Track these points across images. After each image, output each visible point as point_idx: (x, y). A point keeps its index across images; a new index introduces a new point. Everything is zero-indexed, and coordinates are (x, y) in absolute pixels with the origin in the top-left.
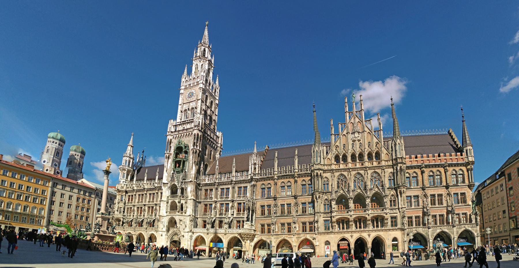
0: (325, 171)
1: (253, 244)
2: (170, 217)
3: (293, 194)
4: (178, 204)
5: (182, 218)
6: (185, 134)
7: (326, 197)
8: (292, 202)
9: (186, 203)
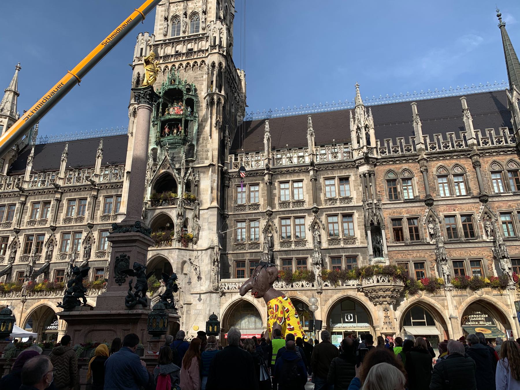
1: (398, 313)
3: (475, 192)
4: (176, 221)
5: (186, 255)
6: (184, 64)
8: (474, 210)
9: (197, 217)
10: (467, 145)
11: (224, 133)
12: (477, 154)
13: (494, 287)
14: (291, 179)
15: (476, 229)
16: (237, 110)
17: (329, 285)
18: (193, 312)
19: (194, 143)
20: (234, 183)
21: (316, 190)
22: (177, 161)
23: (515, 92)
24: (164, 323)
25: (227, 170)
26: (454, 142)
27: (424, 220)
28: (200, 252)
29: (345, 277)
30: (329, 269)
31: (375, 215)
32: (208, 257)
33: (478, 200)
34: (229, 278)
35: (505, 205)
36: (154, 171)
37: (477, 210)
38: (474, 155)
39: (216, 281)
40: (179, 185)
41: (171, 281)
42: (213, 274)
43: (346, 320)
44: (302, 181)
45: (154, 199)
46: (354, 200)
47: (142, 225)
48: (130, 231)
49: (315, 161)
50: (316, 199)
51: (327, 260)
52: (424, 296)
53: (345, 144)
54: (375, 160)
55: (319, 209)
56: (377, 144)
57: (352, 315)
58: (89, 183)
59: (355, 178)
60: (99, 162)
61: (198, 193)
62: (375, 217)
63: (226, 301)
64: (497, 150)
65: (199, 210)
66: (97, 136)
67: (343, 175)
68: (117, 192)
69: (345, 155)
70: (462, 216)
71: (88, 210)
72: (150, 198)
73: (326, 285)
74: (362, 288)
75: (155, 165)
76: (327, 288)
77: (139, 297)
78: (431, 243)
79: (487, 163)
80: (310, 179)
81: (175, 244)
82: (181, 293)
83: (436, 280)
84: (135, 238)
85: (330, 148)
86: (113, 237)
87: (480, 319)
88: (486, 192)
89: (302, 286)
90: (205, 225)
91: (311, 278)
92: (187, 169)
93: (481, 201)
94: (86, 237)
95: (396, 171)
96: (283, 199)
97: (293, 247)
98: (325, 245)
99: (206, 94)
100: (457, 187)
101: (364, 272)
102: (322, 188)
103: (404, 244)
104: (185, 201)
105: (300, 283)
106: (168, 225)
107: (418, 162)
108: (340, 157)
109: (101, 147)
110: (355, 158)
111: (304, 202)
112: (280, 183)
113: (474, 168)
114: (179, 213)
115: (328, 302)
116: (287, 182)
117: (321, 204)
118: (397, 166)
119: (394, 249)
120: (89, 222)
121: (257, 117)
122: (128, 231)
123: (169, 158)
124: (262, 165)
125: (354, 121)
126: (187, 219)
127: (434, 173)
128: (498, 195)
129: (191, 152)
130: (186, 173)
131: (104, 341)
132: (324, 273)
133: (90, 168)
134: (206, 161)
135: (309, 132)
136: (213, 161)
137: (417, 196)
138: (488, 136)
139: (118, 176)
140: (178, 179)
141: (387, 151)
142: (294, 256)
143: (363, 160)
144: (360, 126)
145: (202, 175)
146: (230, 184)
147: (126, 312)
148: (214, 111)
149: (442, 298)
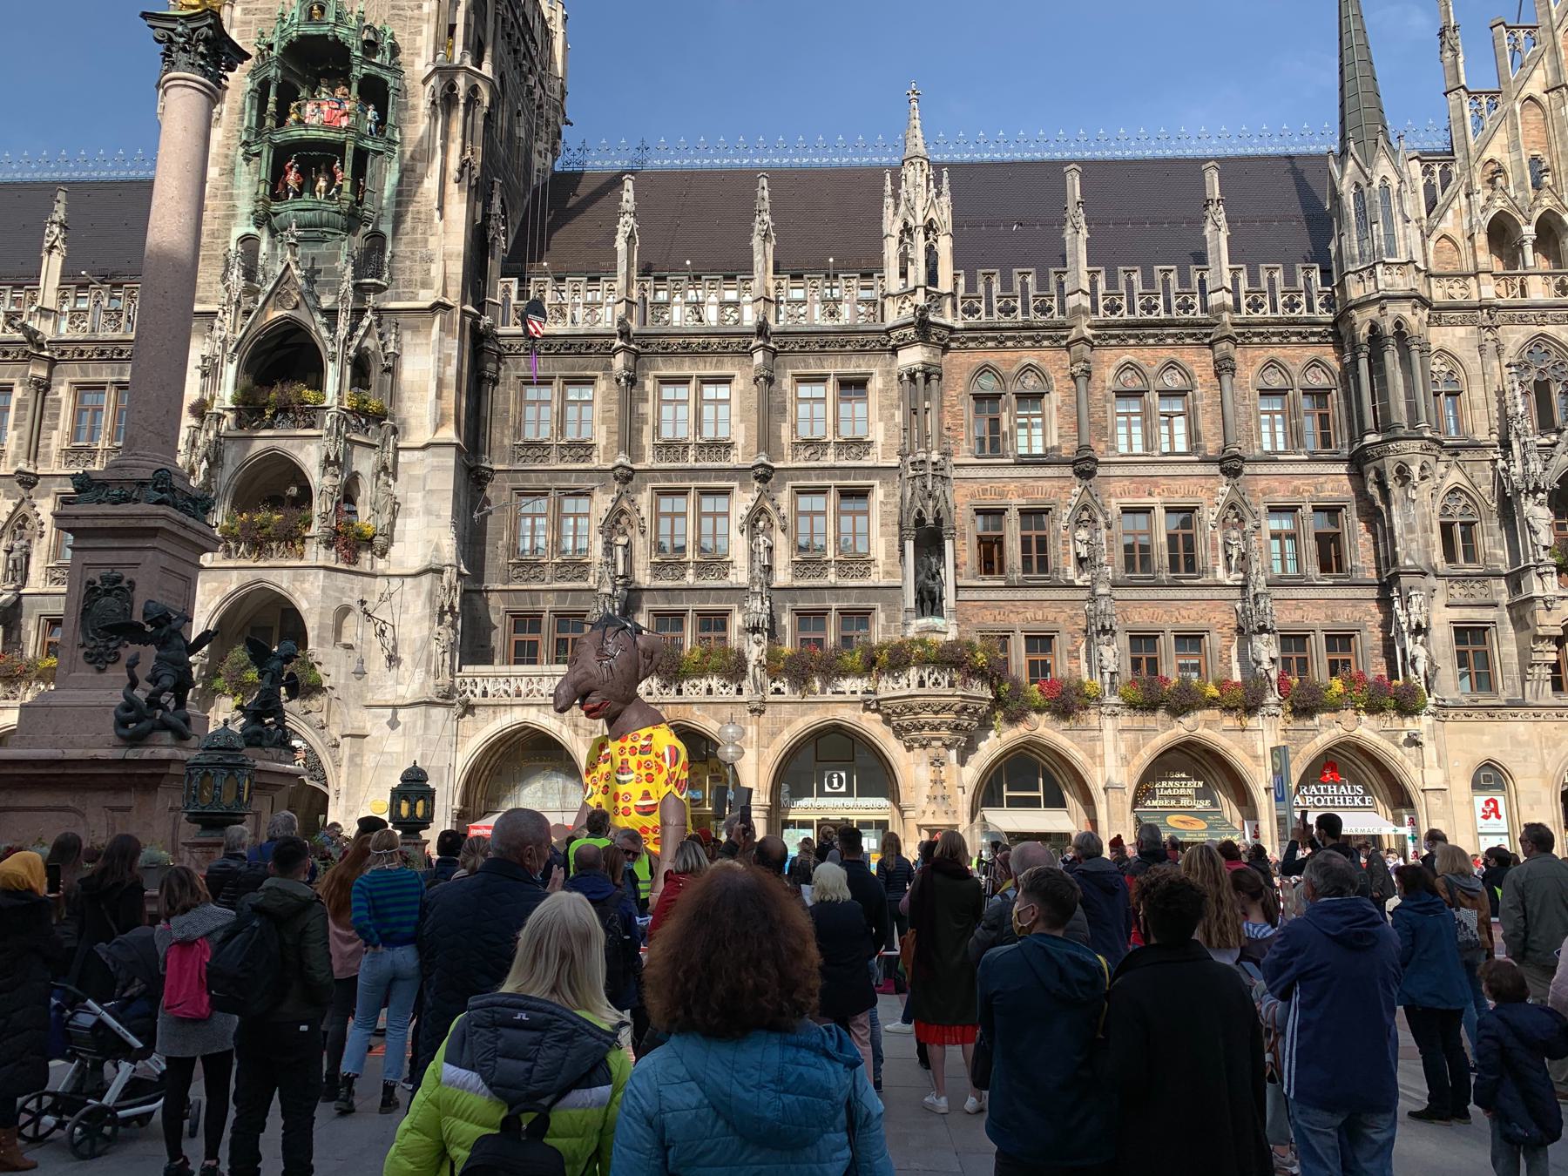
0: (1439, 313)
2: (233, 582)
3: (1212, 446)
4: (318, 479)
5: (351, 589)
7: (1455, 477)
8: (1203, 497)
9: (389, 470)
10: (1205, 309)
11: (487, 205)
12: (1228, 337)
13: (1228, 709)
14: (695, 373)
15: (1201, 551)
16: (533, 134)
17: (786, 689)
18: (369, 760)
19: (386, 228)
20: (512, 371)
21: (769, 412)
22: (327, 283)
23: (1351, 163)
24: (240, 788)
25: (492, 326)
26: (1173, 296)
27: (1065, 518)
28: (396, 582)
29: (832, 670)
30: (788, 647)
31: (930, 496)
32: (423, 596)
33: (1215, 469)
34: (491, 662)
35: (1283, 487)
36: (248, 313)
37: (1210, 496)
38: (1221, 339)
39: (447, 671)
40: (330, 365)
41: (275, 665)
42: (436, 648)
43: (827, 789)
44: (729, 382)
45: (246, 404)
46: (877, 450)
47: (177, 483)
48: (136, 501)
49: (771, 321)
50: (766, 439)
51: (786, 620)
52: (1045, 728)
53: (863, 276)
54: (946, 333)
55: (773, 469)
56: (956, 285)
57: (843, 775)
58: (19, 336)
59: (886, 384)
60: (52, 267)
61: (394, 394)
62: (931, 503)
63: (477, 729)
64: (1282, 329)
65: (397, 449)
66: (46, 176)
67: (851, 370)
68: (121, 374)
69: (862, 309)
70: (1169, 510)
71: (15, 427)
72: (233, 402)
73: (778, 691)
74: (878, 702)
75: (251, 291)
76: (778, 698)
77: (164, 708)
78: (1078, 582)
79: (1254, 363)
80: (753, 375)
81: (316, 553)
82: (334, 702)
83: (1081, 684)
84: (152, 524)
85: (819, 283)
86: (77, 517)
87: (1182, 792)
88: (1241, 447)
89: (709, 691)
90: (415, 501)
91: (735, 670)
92: (359, 313)
93: (1224, 471)
94: (11, 516)
95: (1003, 369)
96: (667, 433)
97: (690, 579)
98: (782, 577)
99: (430, 68)
100: (1165, 429)
101: (885, 658)
102: (788, 406)
103: (1002, 583)
104: (349, 417)
105: (703, 684)
106: (294, 491)
107: (1068, 347)
108: (846, 316)
109: (60, 214)
110: (889, 323)
111: (729, 446)
112: (662, 383)
113: (1218, 375)
114: (328, 456)
115: (779, 738)
116: (684, 381)
117: (781, 457)
118: (1007, 355)
119: (975, 595)
120: (22, 465)
121: (599, 163)
122: (126, 499)
123: (297, 272)
124: (607, 319)
125: (897, 206)
126: (354, 478)
127: (1109, 384)
128: (1270, 459)
129: (372, 260)
130: (354, 328)
131: (40, 842)
132: (772, 656)
133: (21, 287)
134: (422, 293)
135: (757, 227)
136: (445, 294)
137: (1053, 449)
138: (1265, 285)
139: (123, 320)
140: (329, 345)
141: (983, 306)
142: (691, 606)
143: (912, 330)
144: (911, 221)
145: (407, 337)
146: (502, 373)
147: (119, 754)
148: (457, 128)
149: (1092, 734)
